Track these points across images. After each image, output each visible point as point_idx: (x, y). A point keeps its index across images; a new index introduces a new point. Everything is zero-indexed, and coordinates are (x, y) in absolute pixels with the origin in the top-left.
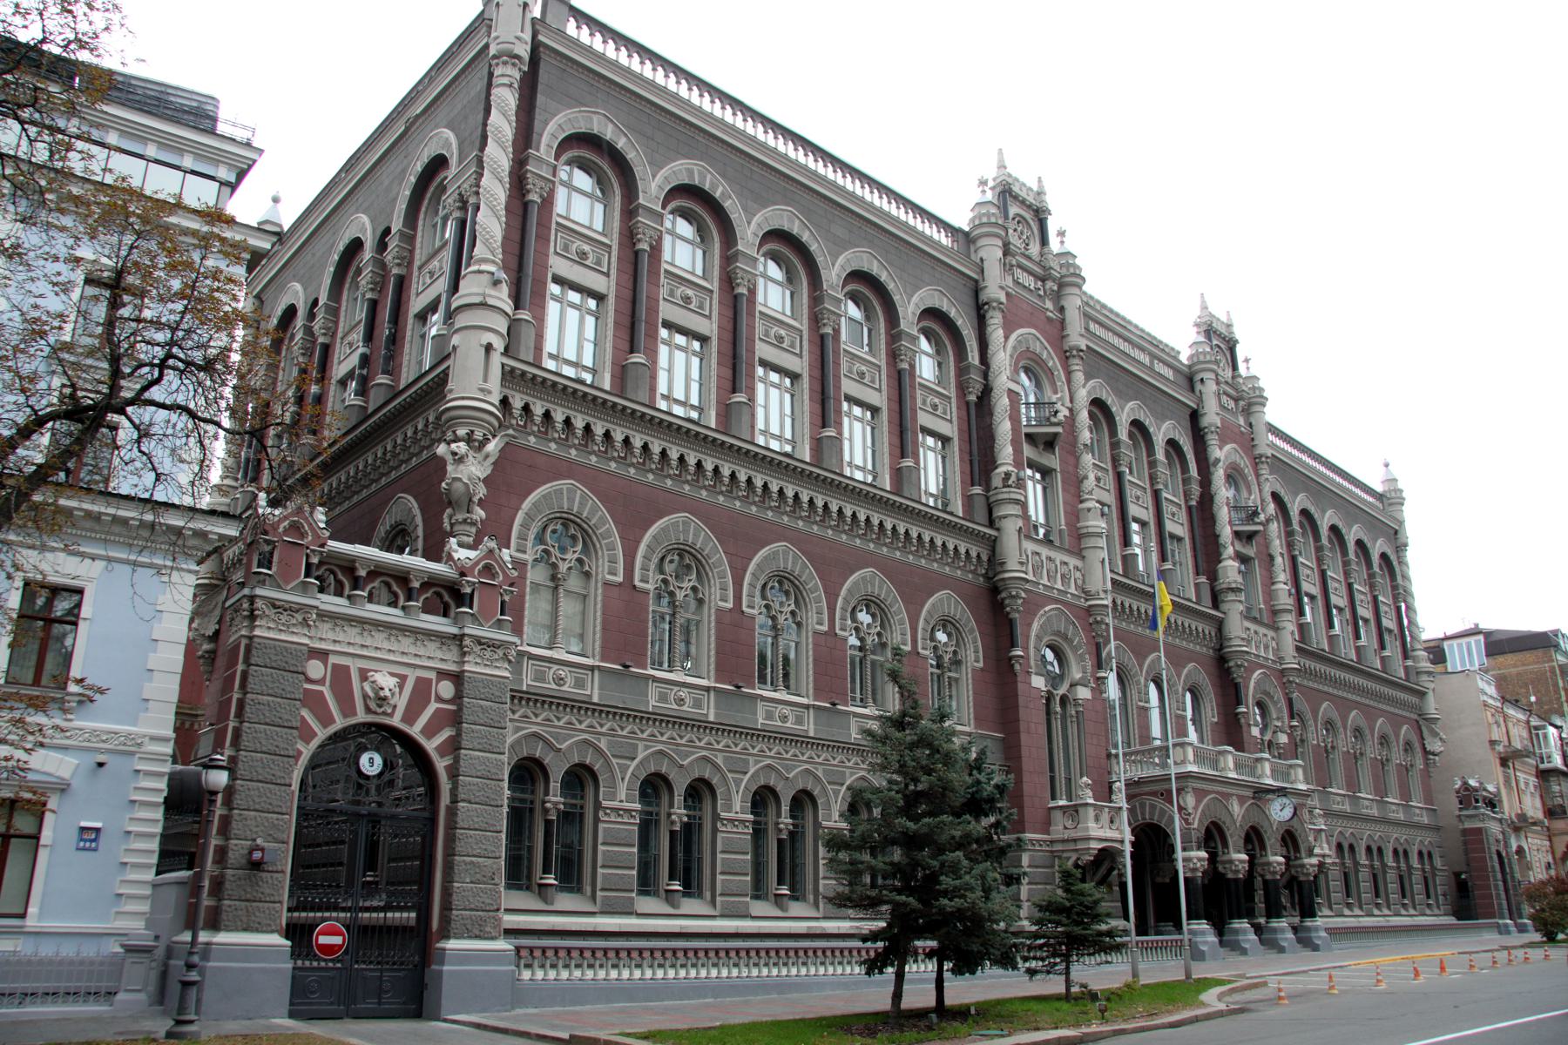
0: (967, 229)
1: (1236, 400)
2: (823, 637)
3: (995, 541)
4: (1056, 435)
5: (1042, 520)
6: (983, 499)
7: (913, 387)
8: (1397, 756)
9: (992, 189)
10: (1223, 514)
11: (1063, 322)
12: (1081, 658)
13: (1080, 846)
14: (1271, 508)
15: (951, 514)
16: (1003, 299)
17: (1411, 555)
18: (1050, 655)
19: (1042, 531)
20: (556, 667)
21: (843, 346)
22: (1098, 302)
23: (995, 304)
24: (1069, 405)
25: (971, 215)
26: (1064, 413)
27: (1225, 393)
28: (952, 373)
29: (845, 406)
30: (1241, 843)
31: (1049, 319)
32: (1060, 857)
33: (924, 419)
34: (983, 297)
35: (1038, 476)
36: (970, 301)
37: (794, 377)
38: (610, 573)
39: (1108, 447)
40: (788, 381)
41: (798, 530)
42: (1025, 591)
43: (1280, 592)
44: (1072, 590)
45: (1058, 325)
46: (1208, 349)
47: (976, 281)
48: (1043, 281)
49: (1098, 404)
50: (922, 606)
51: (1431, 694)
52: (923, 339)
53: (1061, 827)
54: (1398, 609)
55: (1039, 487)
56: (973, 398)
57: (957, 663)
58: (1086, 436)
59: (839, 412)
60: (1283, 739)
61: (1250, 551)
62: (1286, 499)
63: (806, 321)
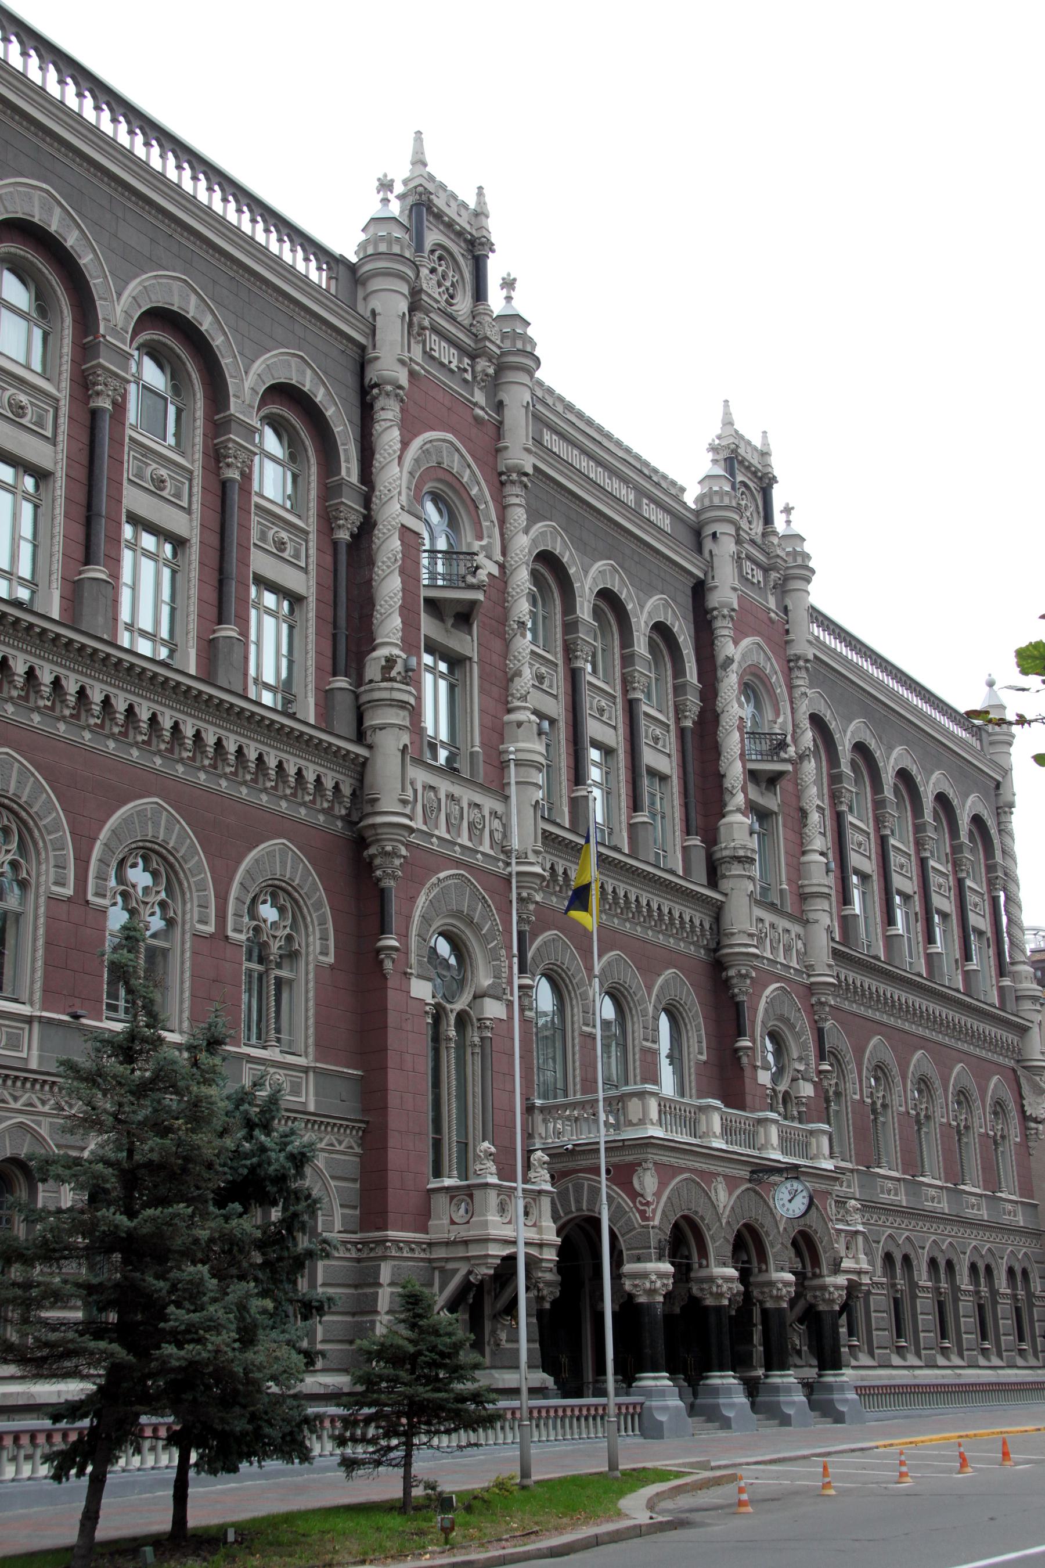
0: (354, 259)
1: (766, 570)
2: (64, 907)
3: (364, 764)
4: (473, 603)
5: (444, 735)
6: (349, 699)
7: (245, 510)
8: (982, 1122)
9: (401, 197)
10: (732, 742)
11: (499, 426)
12: (493, 956)
13: (474, 1251)
14: (808, 737)
15: (292, 716)
16: (404, 379)
17: (1019, 821)
18: (443, 948)
19: (443, 754)
21: (129, 432)
22: (561, 399)
23: (389, 388)
24: (500, 559)
25: (363, 237)
26: (489, 568)
27: (749, 557)
28: (313, 494)
29: (128, 531)
30: (728, 1250)
31: (477, 419)
32: (442, 1270)
33: (261, 563)
34: (372, 375)
35: (443, 667)
36: (350, 380)
37: (41, 476)
39: (559, 630)
40: (29, 483)
41: (32, 730)
42: (408, 845)
43: (813, 867)
44: (486, 848)
45: (491, 431)
46: (727, 488)
47: (363, 348)
48: (473, 357)
49: (547, 559)
50: (239, 862)
51: (1036, 1029)
52: (269, 434)
53: (446, 1221)
54: (995, 901)
55: (443, 685)
56: (344, 535)
57: (291, 956)
58: (522, 608)
59: (116, 539)
60: (807, 1090)
61: (771, 802)
62: (833, 726)
63: (65, 384)
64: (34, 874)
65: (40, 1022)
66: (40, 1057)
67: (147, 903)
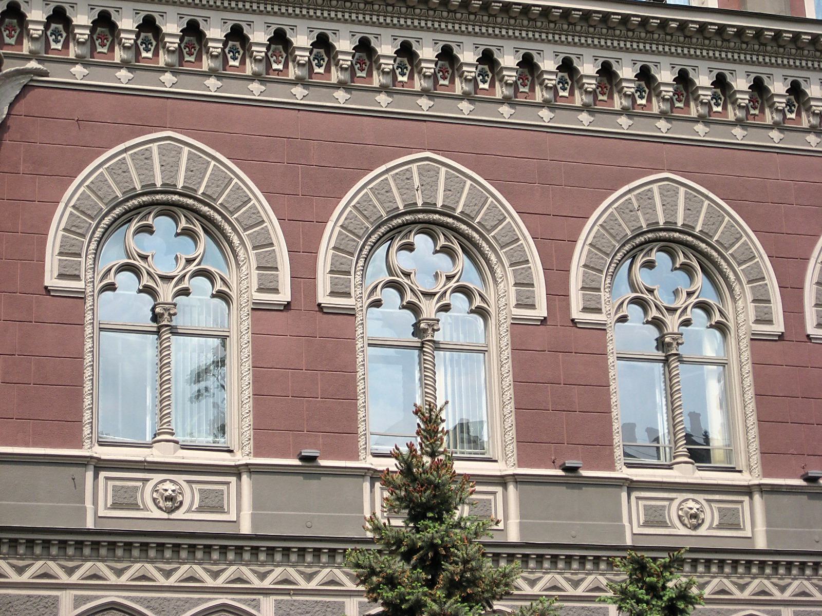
20: (157, 477)
38: (260, 290)
64: (731, 316)
65: (250, 472)
66: (768, 533)
67: (675, 310)
